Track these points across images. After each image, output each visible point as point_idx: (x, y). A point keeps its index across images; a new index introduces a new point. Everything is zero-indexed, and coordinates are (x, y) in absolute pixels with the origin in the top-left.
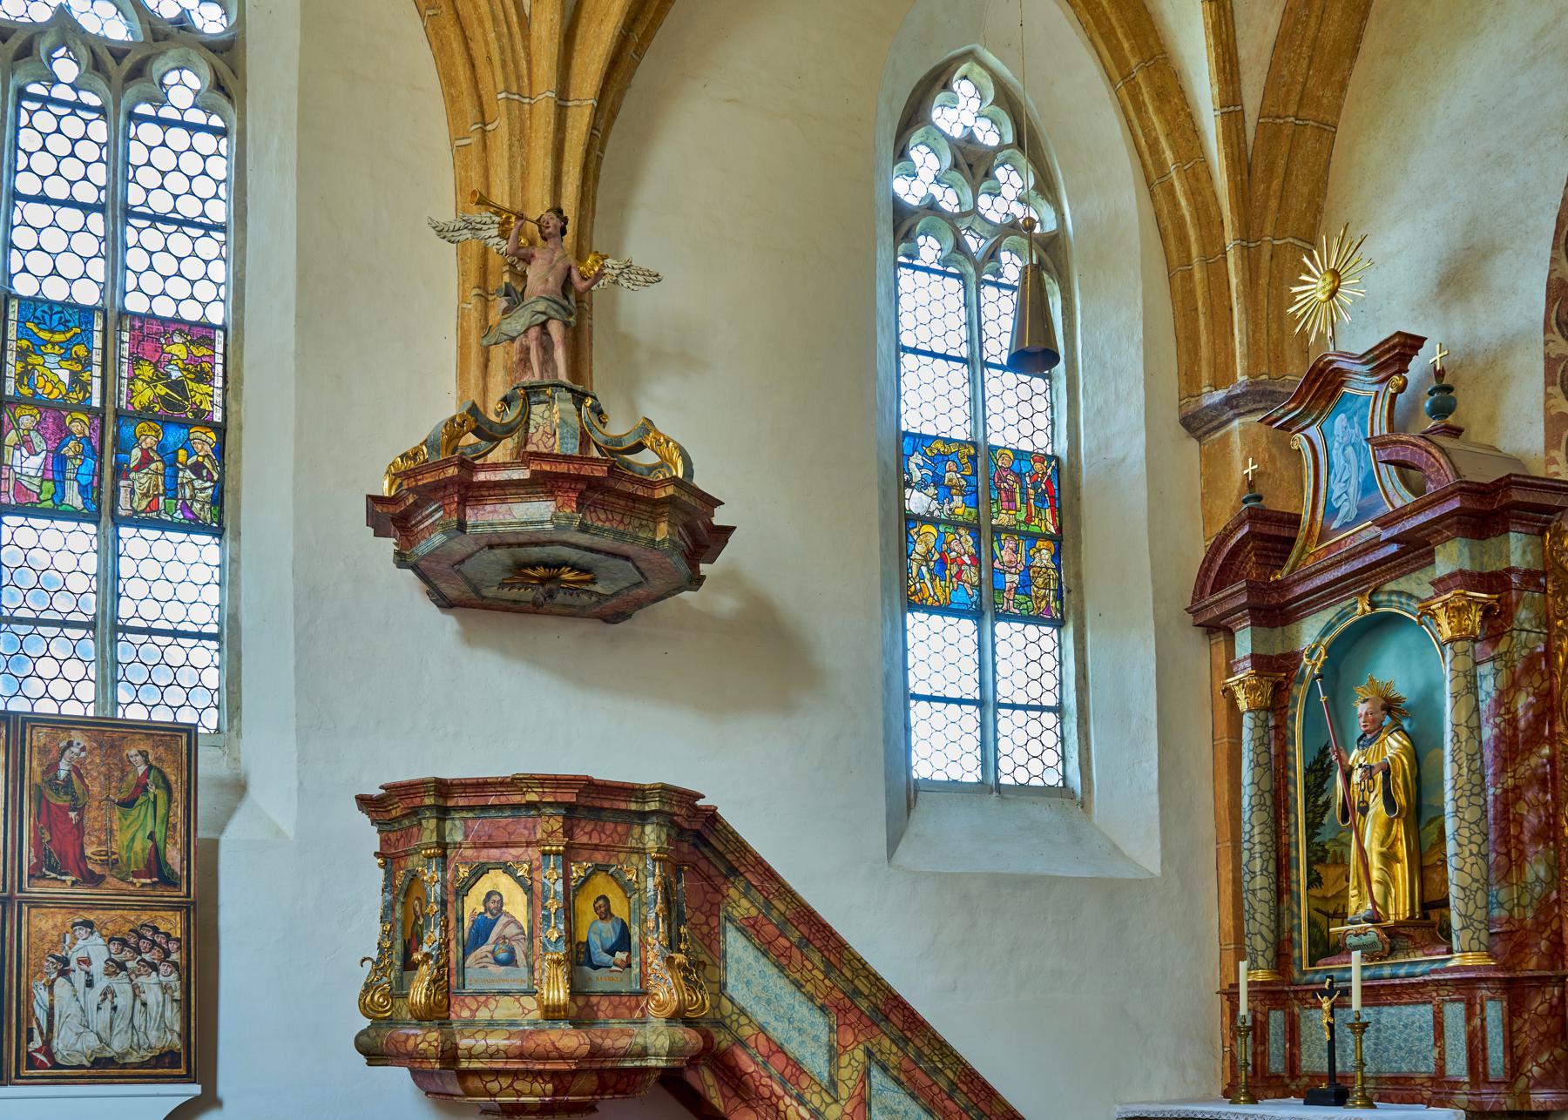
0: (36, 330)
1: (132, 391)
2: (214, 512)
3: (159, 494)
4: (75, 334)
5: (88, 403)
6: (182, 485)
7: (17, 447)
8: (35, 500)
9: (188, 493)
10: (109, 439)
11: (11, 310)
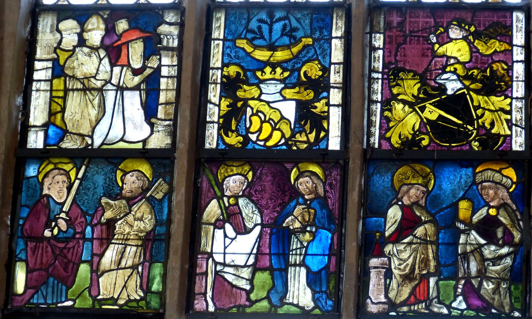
0: (249, 49)
1: (388, 120)
2: (517, 293)
3: (430, 275)
4: (305, 47)
5: (322, 146)
6: (465, 256)
7: (219, 224)
8: (243, 301)
9: (474, 267)
10: (354, 197)
11: (215, 25)
